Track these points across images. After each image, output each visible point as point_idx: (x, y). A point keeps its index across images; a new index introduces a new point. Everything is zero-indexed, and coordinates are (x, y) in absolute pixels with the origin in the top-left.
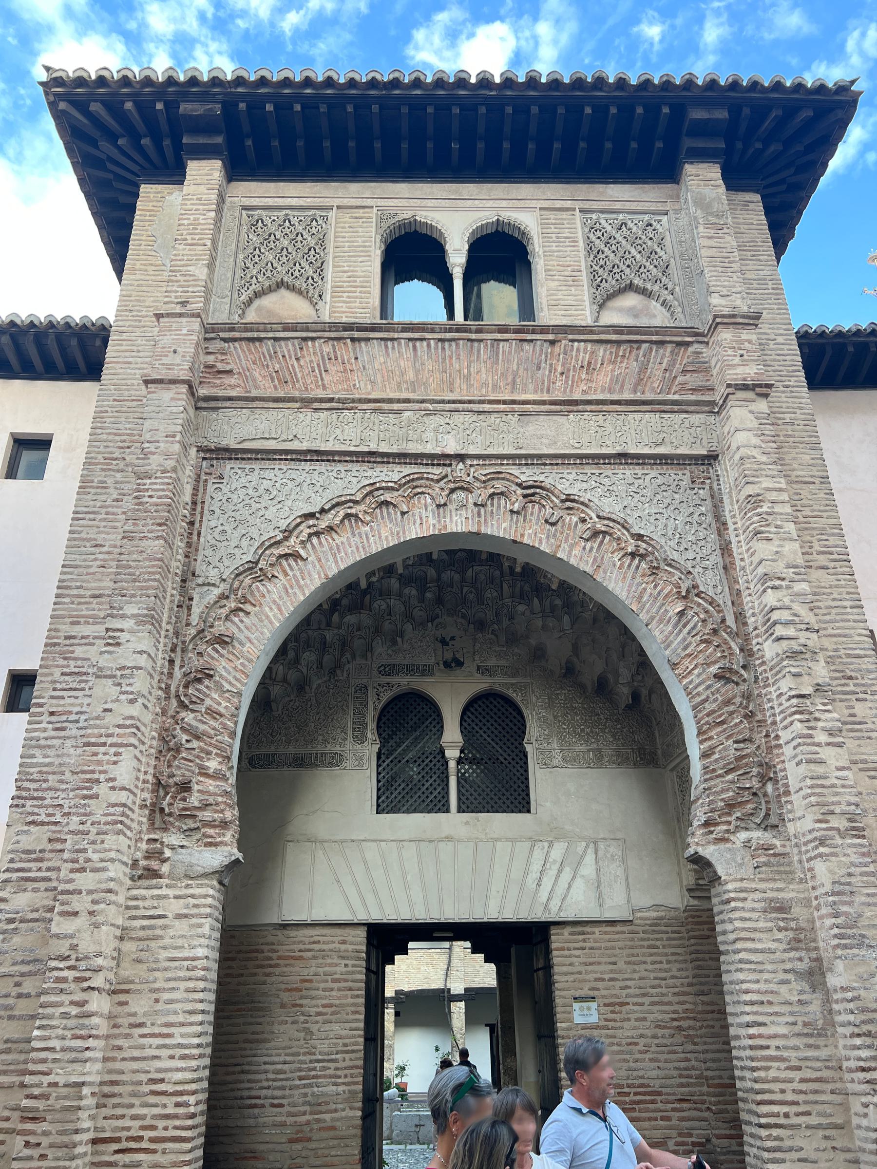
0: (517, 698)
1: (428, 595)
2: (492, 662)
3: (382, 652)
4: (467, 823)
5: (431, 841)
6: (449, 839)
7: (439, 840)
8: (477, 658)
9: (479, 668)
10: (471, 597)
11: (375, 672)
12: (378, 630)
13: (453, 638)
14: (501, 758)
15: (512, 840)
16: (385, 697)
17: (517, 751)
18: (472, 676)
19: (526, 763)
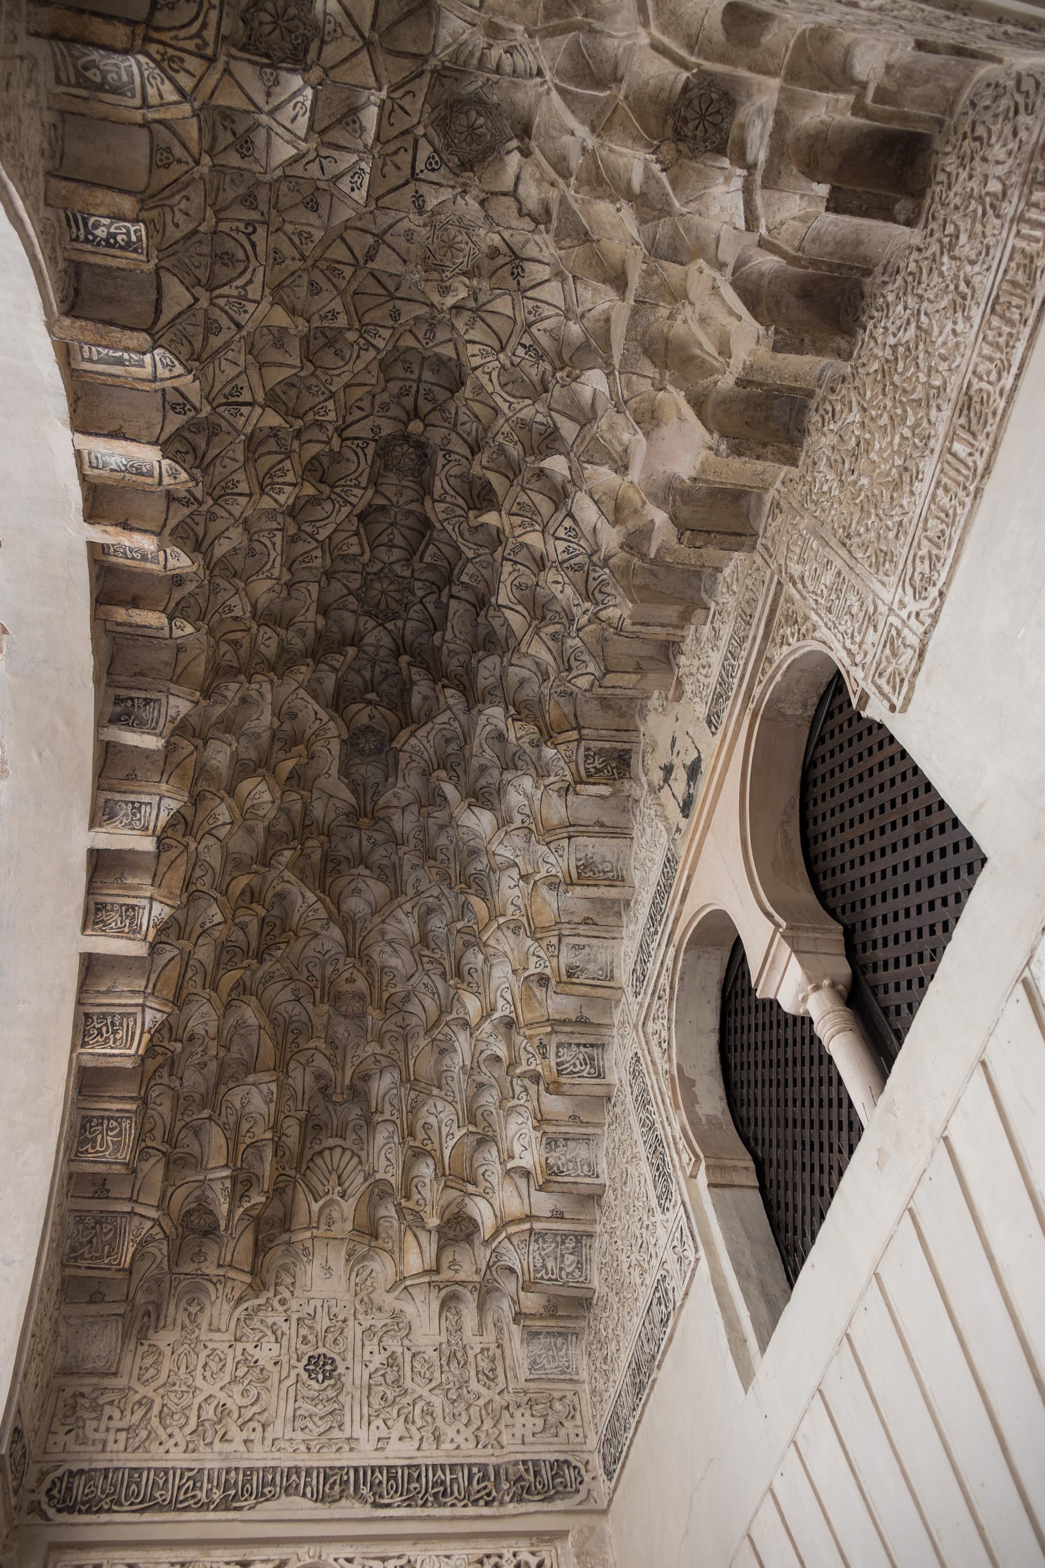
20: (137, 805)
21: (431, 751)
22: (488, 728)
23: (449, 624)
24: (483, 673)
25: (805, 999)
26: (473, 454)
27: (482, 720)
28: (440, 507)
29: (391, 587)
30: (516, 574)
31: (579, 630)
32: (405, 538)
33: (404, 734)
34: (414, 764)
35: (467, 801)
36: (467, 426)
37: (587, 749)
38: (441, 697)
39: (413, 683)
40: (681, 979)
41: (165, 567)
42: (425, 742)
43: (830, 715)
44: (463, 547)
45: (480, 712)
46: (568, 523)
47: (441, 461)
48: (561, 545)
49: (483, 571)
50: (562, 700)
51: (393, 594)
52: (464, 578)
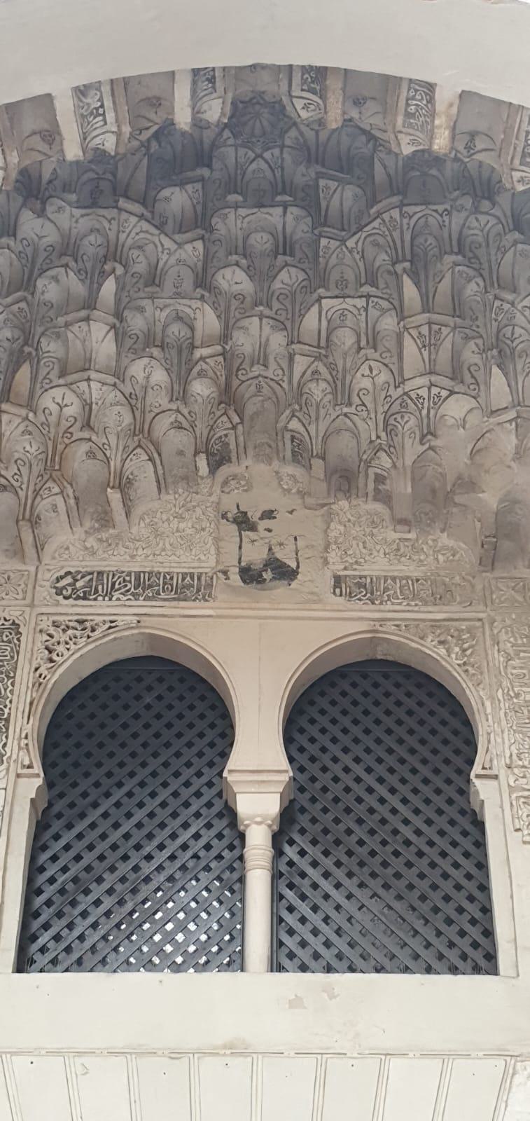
0: (446, 660)
1: (201, 389)
2: (377, 566)
3: (70, 546)
4: (296, 1003)
5: (175, 1055)
6: (236, 1049)
7: (203, 1053)
8: (333, 556)
9: (338, 581)
10: (318, 391)
11: (45, 591)
12: (53, 465)
13: (269, 515)
14: (407, 832)
15: (445, 1056)
16: (77, 659)
17: (451, 811)
18: (320, 601)
19: (481, 844)
20: (101, 111)
21: (130, 241)
22: (188, 310)
23: (255, 210)
24: (228, 272)
25: (259, 823)
26: (460, 252)
27: (198, 304)
28: (395, 213)
29: (265, 123)
30: (356, 312)
31: (346, 415)
32: (329, 139)
33: (137, 208)
34: (107, 225)
35: (115, 321)
36: (475, 224)
37: (226, 436)
38: (189, 235)
39: (182, 184)
40: (115, 639)
41: (401, 132)
42: (137, 229)
43: (386, 676)
44: (357, 236)
45: (202, 298)
46: (444, 393)
47: (440, 208)
48: (424, 392)
49: (334, 256)
50: (253, 388)
51: (258, 124)
52: (324, 242)
